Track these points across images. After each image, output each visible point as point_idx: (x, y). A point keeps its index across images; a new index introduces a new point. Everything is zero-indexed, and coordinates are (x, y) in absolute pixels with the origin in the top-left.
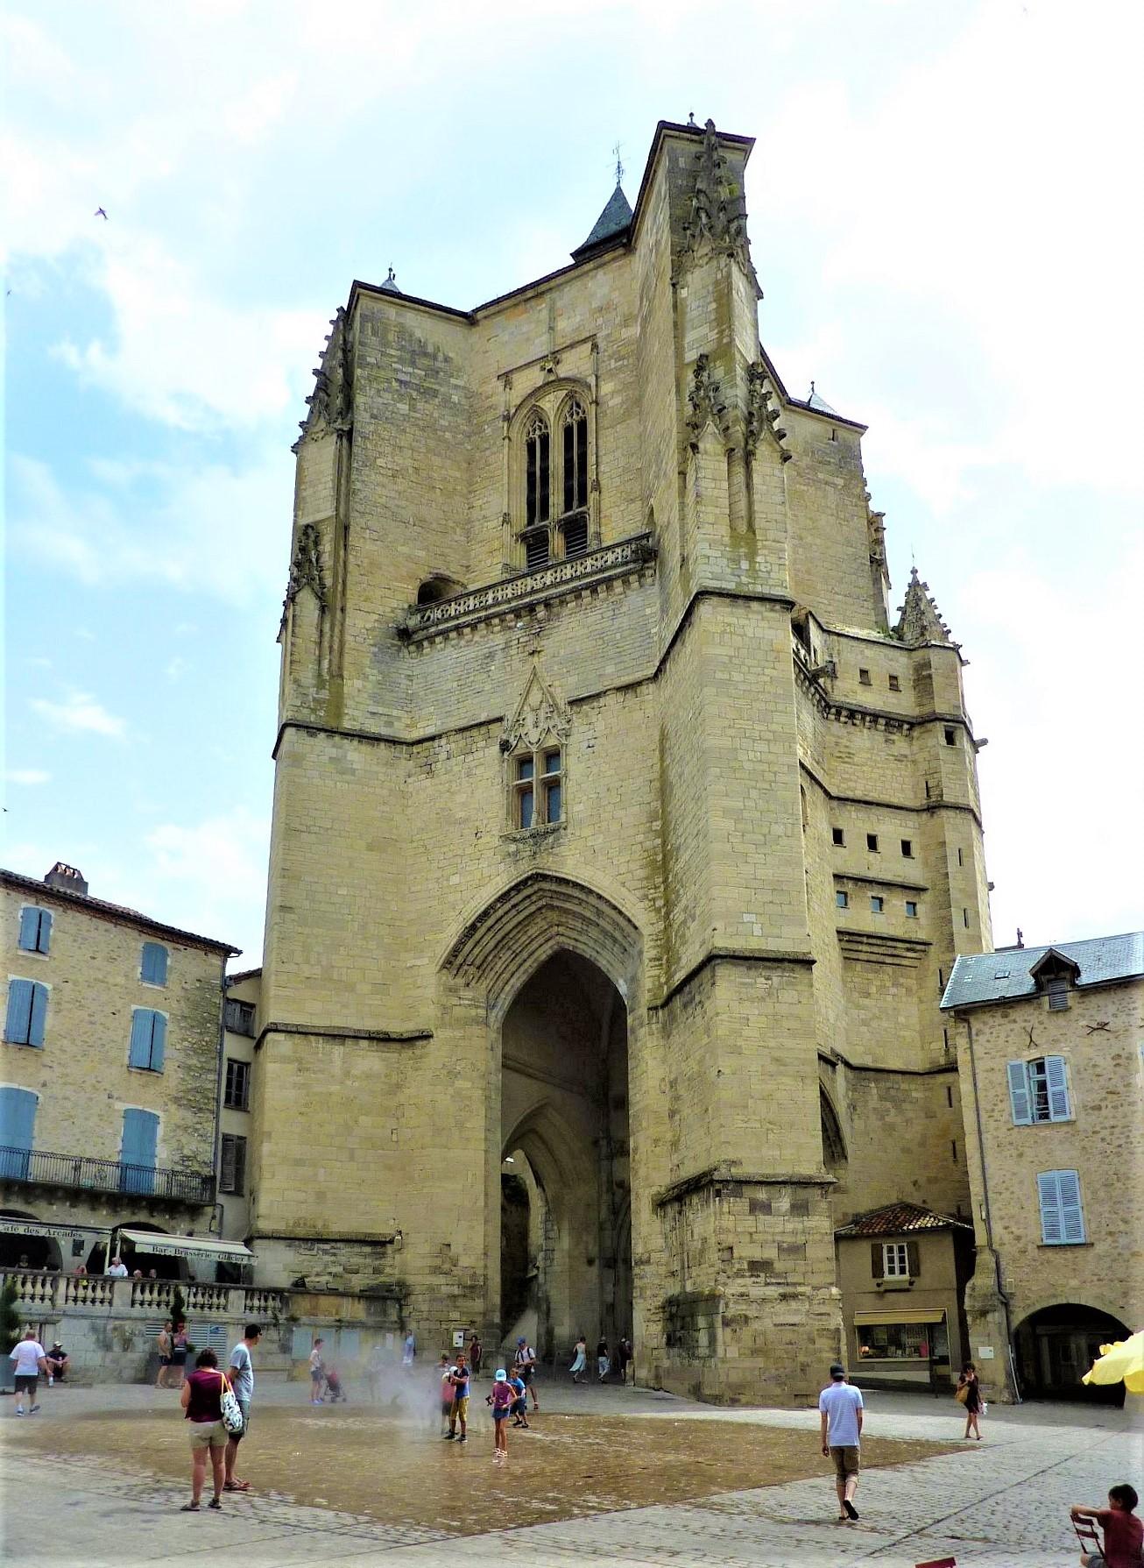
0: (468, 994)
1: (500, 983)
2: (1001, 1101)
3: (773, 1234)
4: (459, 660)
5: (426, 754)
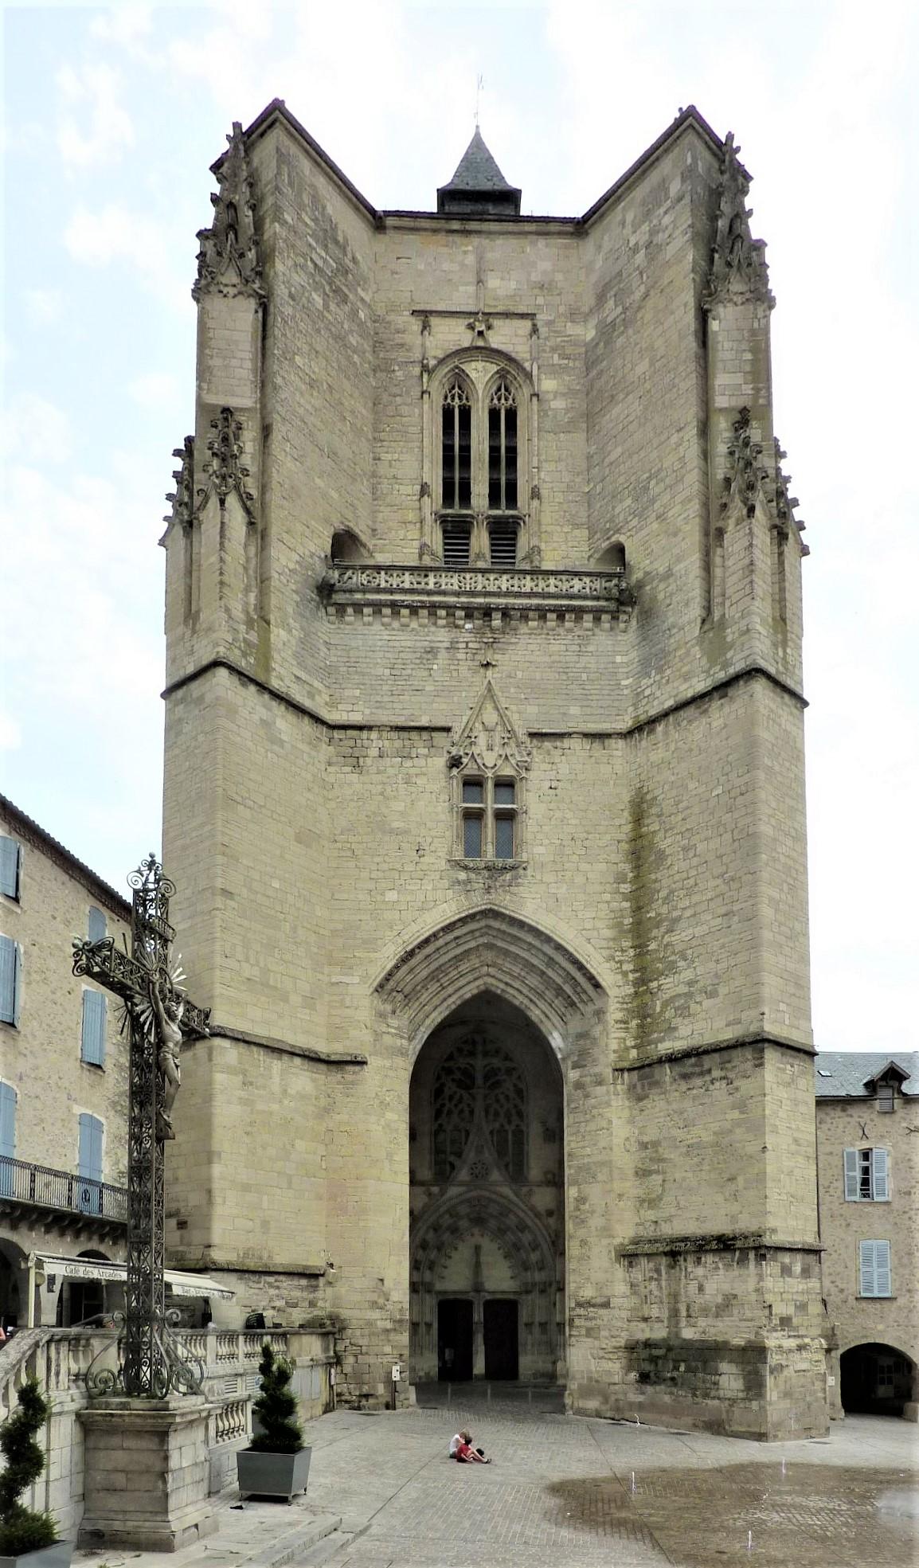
4: (391, 644)
5: (352, 743)
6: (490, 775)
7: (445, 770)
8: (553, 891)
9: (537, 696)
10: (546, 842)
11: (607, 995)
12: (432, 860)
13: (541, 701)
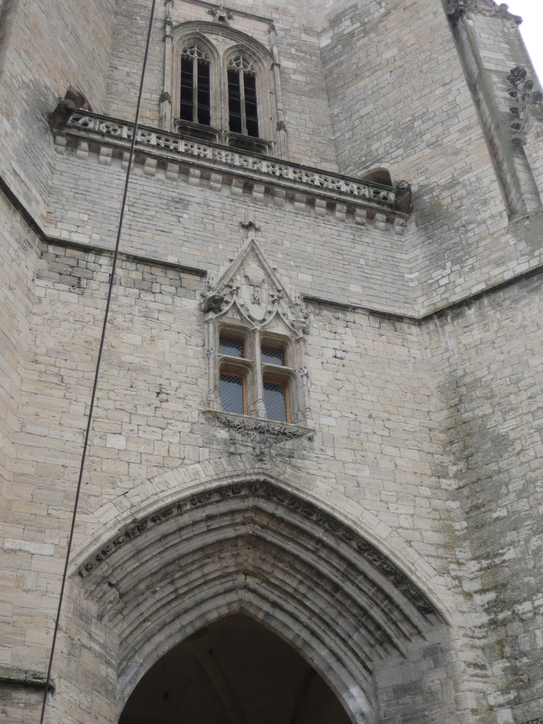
0: (100, 634)
5: (73, 262)
6: (258, 328)
7: (197, 312)
8: (351, 472)
9: (310, 267)
10: (336, 413)
11: (447, 624)
12: (180, 408)
13: (315, 273)
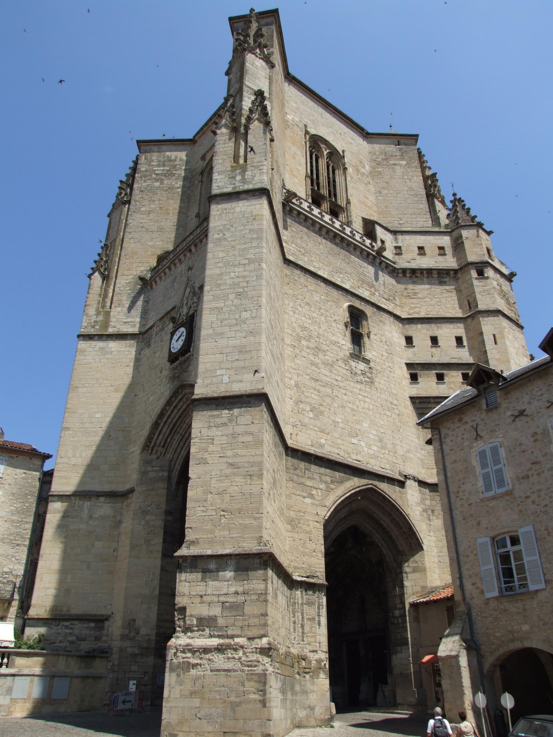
1: (176, 455)
2: (463, 484)
3: (219, 595)
